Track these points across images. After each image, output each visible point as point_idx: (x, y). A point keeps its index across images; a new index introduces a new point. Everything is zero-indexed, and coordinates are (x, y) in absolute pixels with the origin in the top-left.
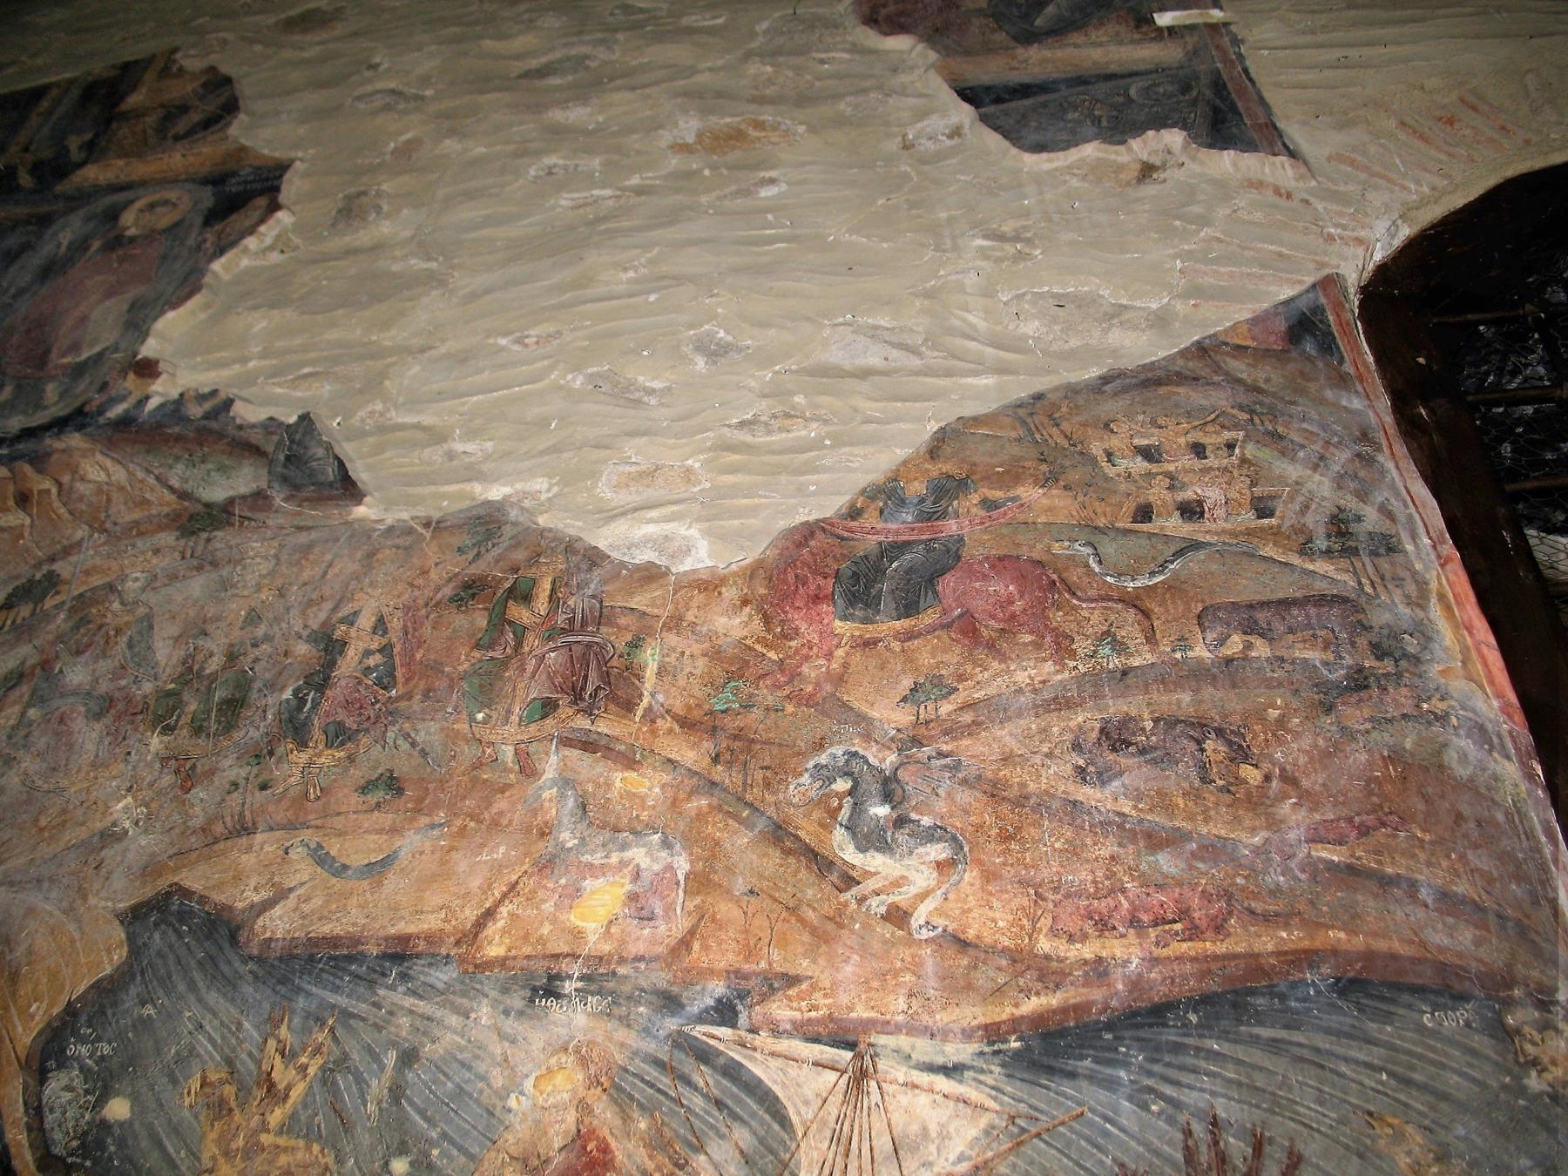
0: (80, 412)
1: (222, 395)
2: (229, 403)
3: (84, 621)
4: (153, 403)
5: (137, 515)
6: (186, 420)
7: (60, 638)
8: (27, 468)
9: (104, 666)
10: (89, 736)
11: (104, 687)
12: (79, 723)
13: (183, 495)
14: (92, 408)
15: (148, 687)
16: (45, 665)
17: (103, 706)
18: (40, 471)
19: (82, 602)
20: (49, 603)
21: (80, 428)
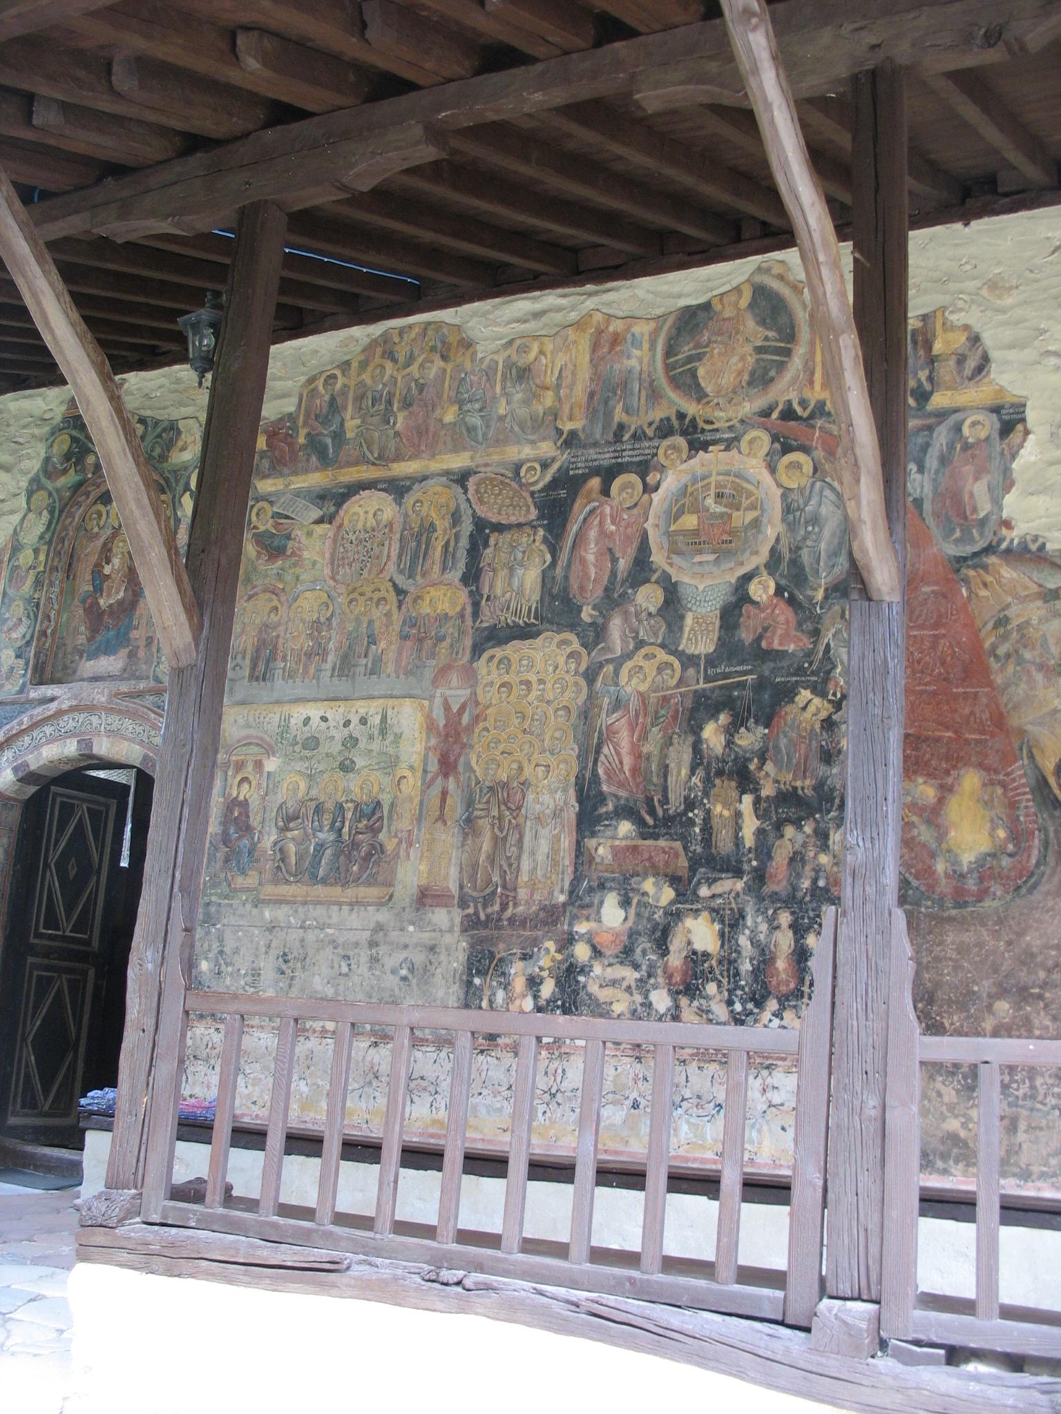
0: (990, 546)
1: (1041, 540)
2: (1044, 545)
3: (1023, 636)
4: (1016, 542)
5: (1026, 593)
6: (1029, 551)
7: (1018, 642)
8: (981, 571)
9: (1036, 653)
10: (1039, 677)
11: (1038, 660)
12: (1034, 673)
13: (1040, 586)
14: (994, 543)
15: (1053, 662)
16: (1016, 651)
17: (1041, 667)
18: (987, 573)
19: (1020, 628)
20: (1009, 627)
21: (994, 553)
